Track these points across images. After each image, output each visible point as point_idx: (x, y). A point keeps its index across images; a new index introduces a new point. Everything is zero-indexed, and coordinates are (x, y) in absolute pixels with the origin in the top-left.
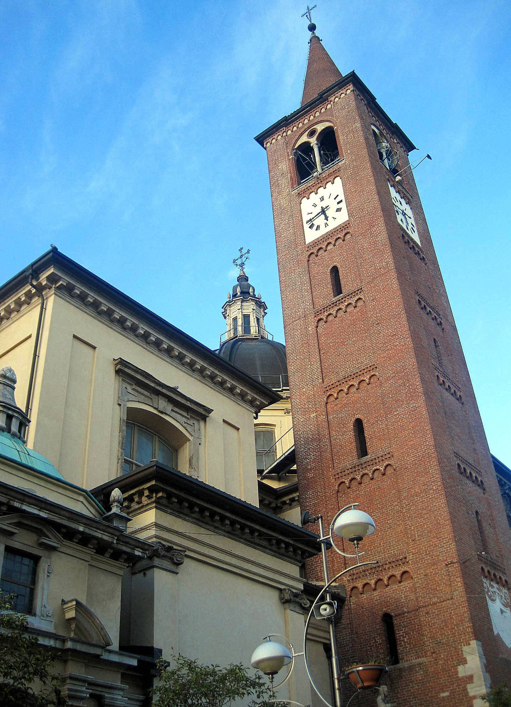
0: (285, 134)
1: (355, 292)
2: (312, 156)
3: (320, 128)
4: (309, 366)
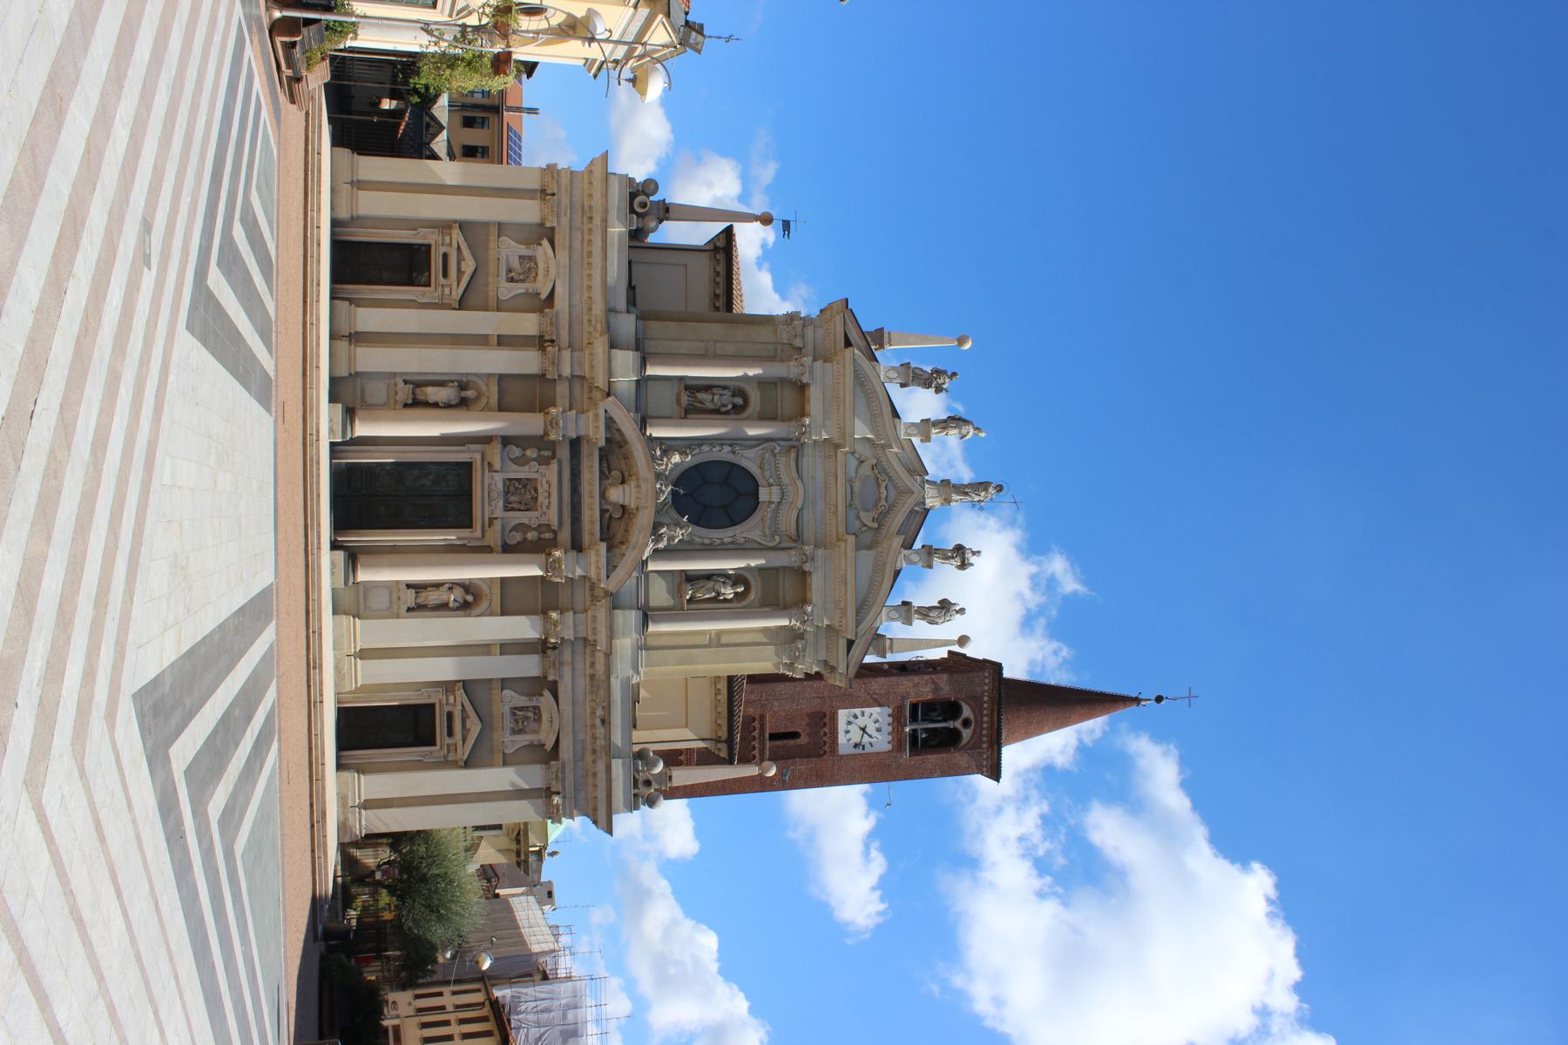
3: (966, 734)
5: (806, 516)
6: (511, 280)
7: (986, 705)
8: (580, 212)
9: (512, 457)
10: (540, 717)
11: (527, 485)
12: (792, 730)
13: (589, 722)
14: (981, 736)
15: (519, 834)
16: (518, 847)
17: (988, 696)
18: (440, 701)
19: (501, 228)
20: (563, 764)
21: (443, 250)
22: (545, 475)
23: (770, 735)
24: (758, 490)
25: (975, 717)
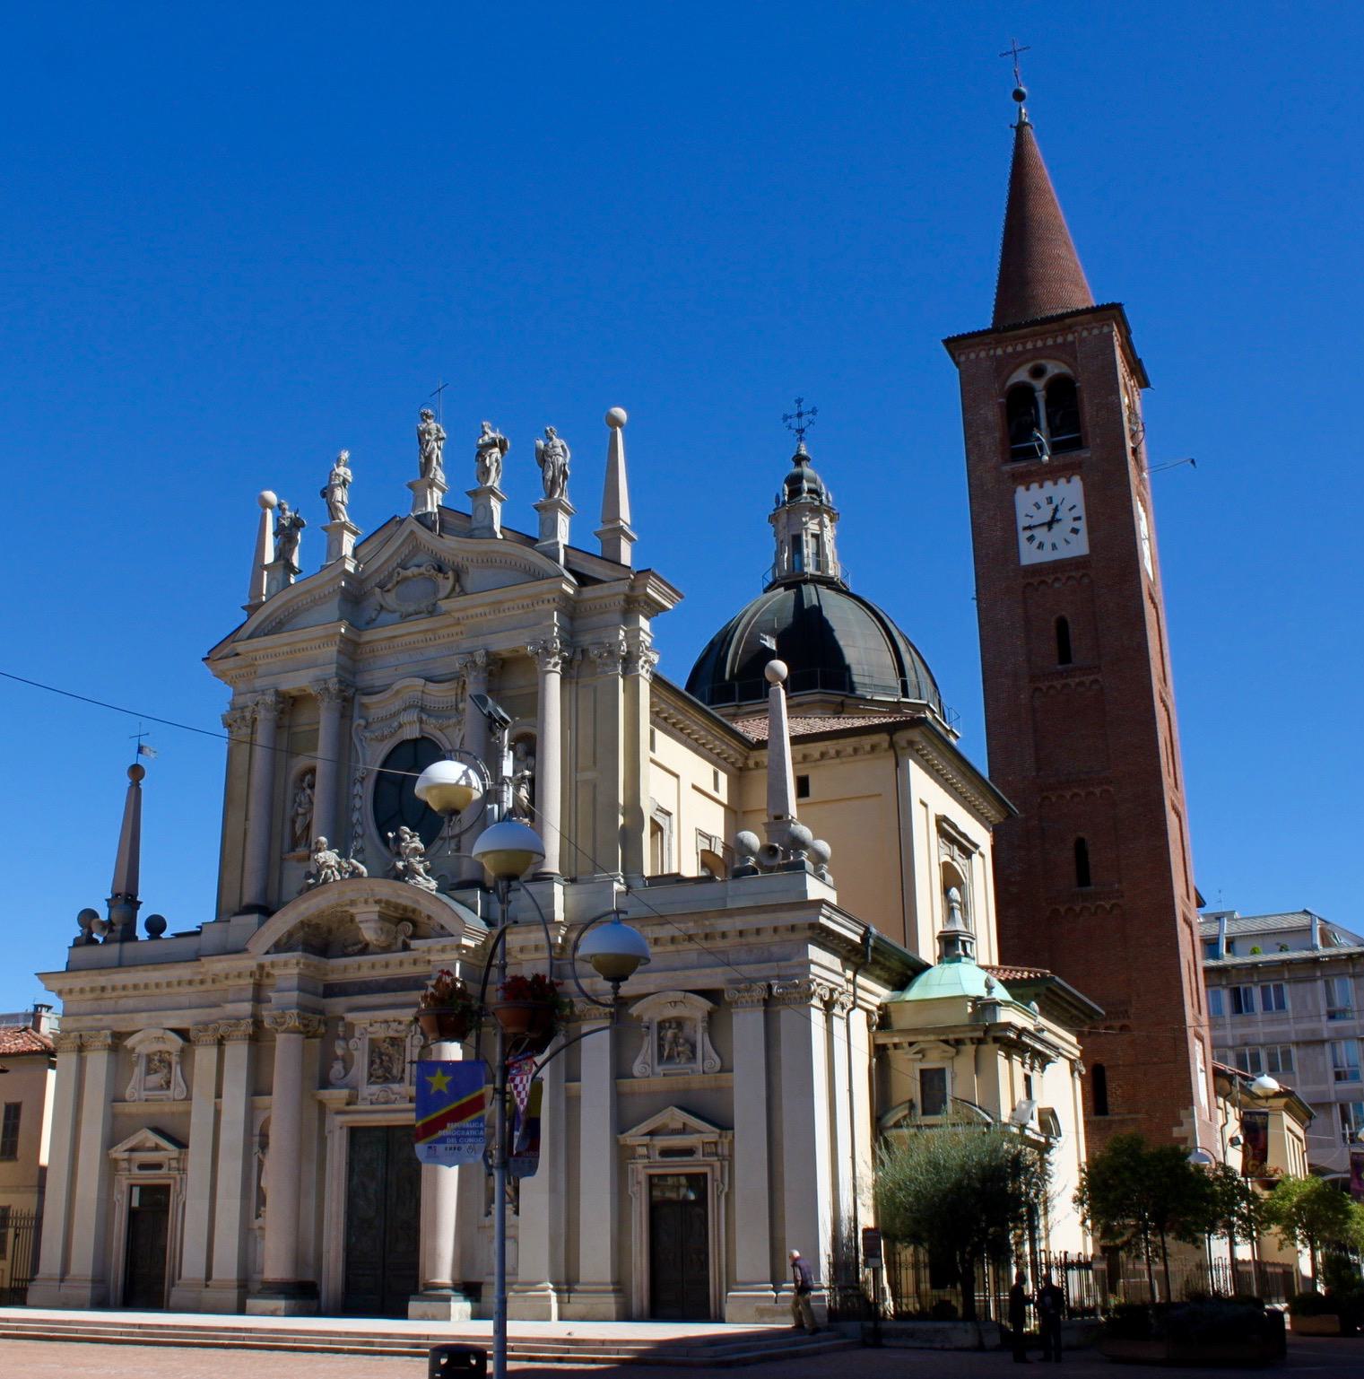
0: (992, 352)
1: (1090, 669)
2: (1033, 411)
3: (1054, 368)
4: (1018, 749)
5: (440, 669)
6: (168, 1083)
7: (1010, 349)
8: (100, 1002)
9: (343, 1074)
10: (669, 1021)
11: (375, 1051)
12: (1053, 632)
13: (671, 948)
14: (1056, 346)
15: (946, 1042)
16: (968, 1042)
17: (995, 349)
18: (646, 1167)
19: (115, 1098)
20: (731, 981)
21: (136, 1171)
22: (365, 1029)
23: (1061, 662)
24: (408, 740)
25: (1027, 361)
